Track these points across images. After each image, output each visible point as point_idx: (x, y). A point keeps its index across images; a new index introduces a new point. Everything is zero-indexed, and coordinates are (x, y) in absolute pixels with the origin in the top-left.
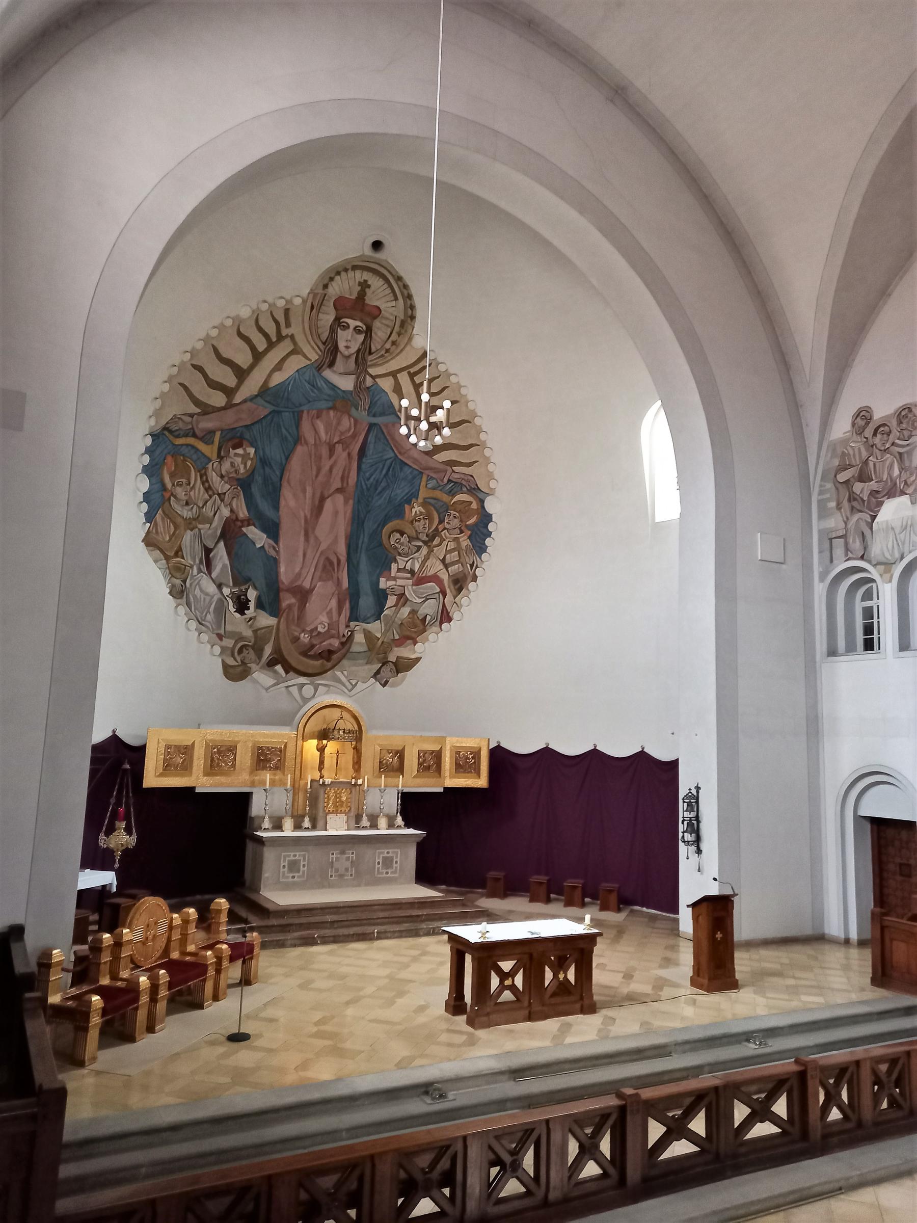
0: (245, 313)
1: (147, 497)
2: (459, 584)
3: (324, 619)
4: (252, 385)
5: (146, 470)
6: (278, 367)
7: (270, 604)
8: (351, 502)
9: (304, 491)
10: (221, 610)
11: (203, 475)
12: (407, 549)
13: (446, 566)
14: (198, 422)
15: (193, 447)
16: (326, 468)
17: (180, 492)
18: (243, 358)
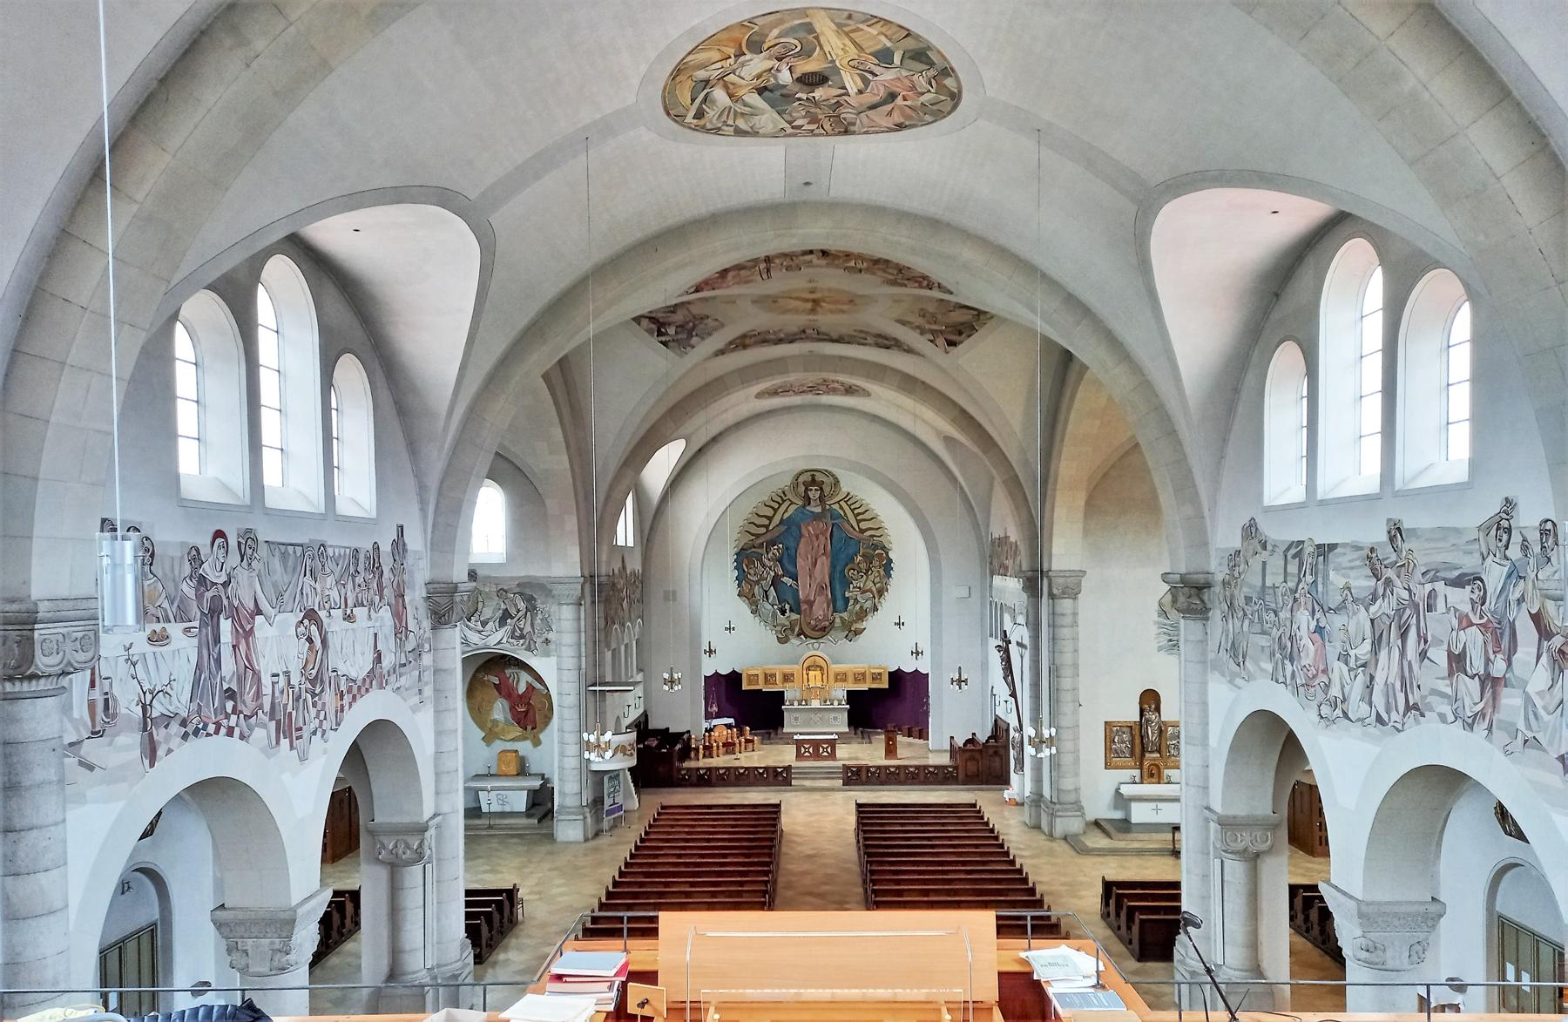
2: (881, 592)
7: (796, 609)
10: (774, 615)
18: (770, 512)
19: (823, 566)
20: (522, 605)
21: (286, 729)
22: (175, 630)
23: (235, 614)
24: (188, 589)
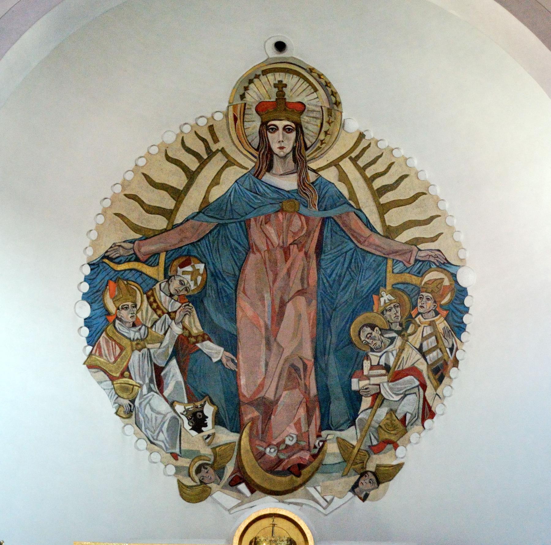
0: (170, 138)
1: (88, 322)
2: (440, 372)
3: (293, 431)
4: (192, 203)
5: (86, 297)
6: (216, 181)
7: (230, 419)
8: (314, 302)
9: (262, 299)
11: (150, 296)
12: (379, 343)
13: (424, 356)
14: (139, 247)
15: (137, 271)
16: (283, 273)
17: (124, 314)
18: (178, 180)
19: (300, 315)
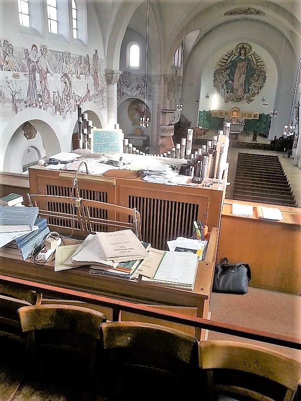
4: (229, 61)
18: (227, 58)
19: (244, 76)
20: (143, 84)
21: (58, 109)
22: (21, 74)
23: (40, 72)
24: (25, 62)
